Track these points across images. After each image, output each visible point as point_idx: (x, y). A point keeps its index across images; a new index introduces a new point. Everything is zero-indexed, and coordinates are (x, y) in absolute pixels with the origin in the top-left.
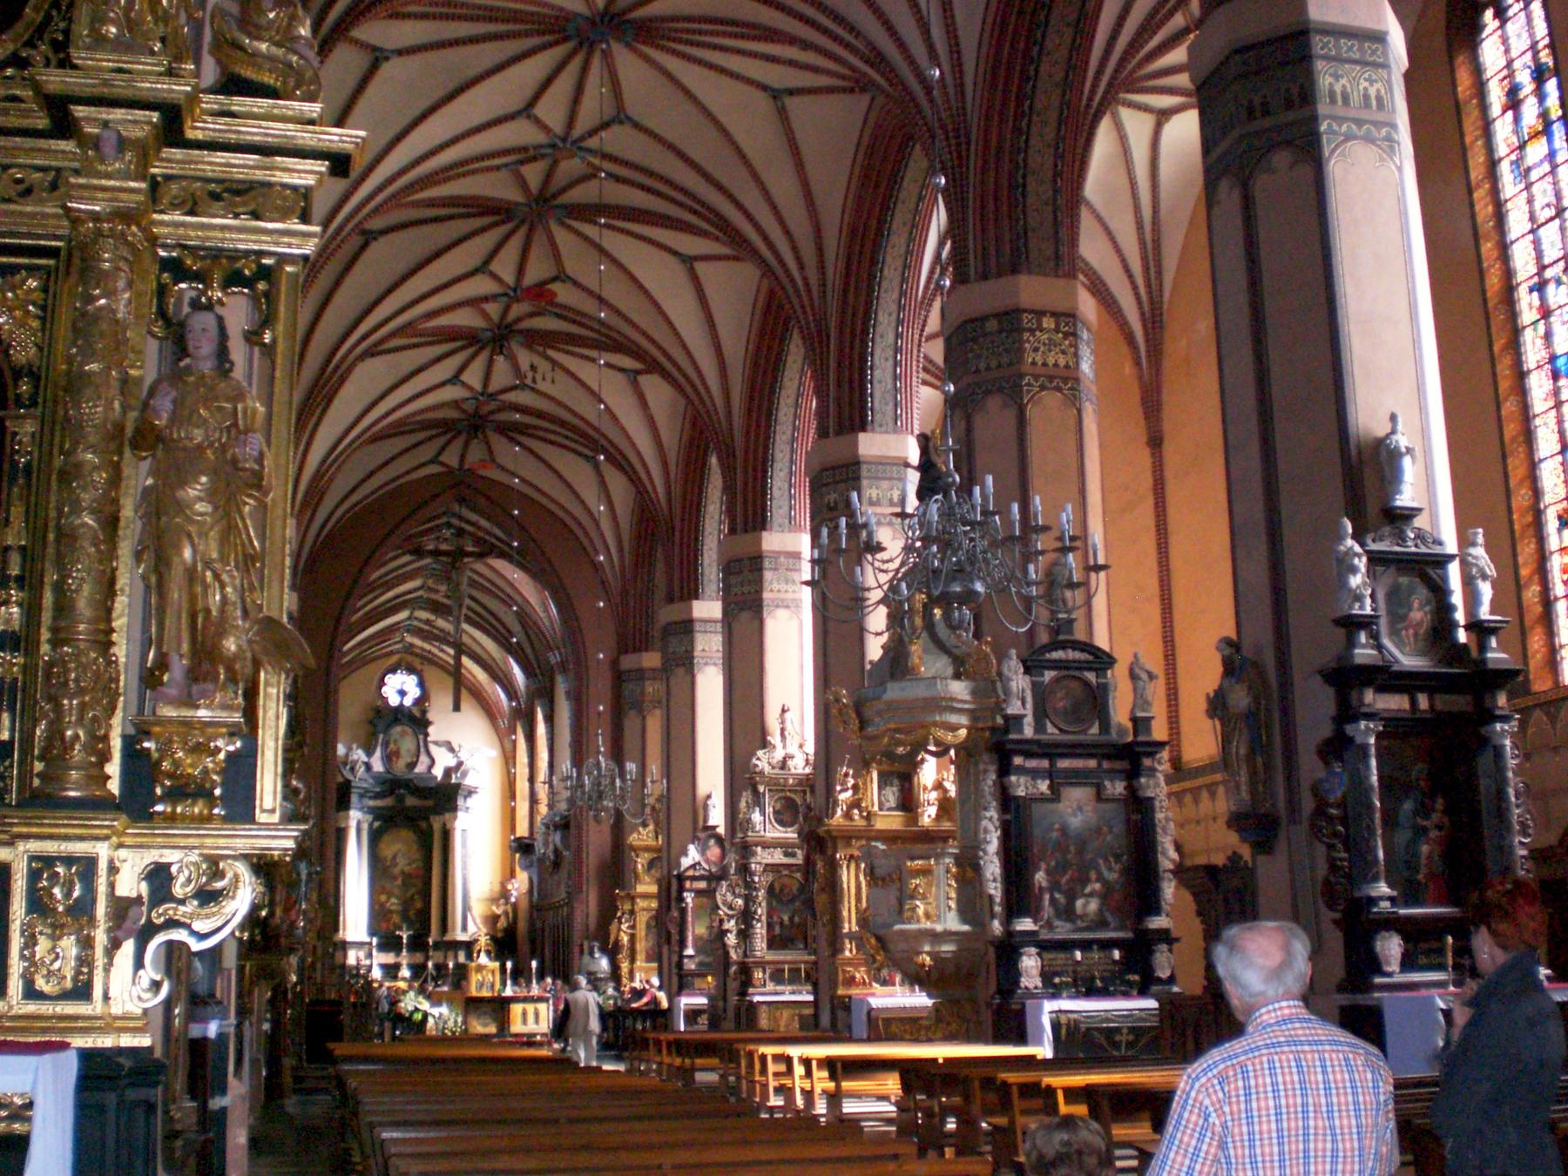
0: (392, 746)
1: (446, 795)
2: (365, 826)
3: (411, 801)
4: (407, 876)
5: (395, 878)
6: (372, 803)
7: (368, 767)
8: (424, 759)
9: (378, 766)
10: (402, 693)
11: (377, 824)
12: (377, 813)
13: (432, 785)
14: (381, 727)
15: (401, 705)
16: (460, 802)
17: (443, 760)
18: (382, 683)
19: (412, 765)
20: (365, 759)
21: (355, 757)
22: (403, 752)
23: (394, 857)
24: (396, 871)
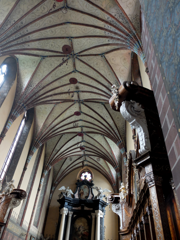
0: (81, 191)
1: (96, 204)
2: (70, 215)
3: (86, 208)
4: (83, 235)
5: (79, 235)
6: (73, 208)
7: (73, 196)
8: (91, 195)
9: (77, 196)
10: (85, 176)
11: (75, 216)
12: (75, 212)
13: (92, 202)
14: (79, 186)
15: (85, 178)
16: (100, 206)
17: (95, 193)
18: (81, 175)
19: (87, 197)
20: (73, 194)
21: (68, 190)
22: (84, 193)
23: (79, 228)
24: (80, 233)
